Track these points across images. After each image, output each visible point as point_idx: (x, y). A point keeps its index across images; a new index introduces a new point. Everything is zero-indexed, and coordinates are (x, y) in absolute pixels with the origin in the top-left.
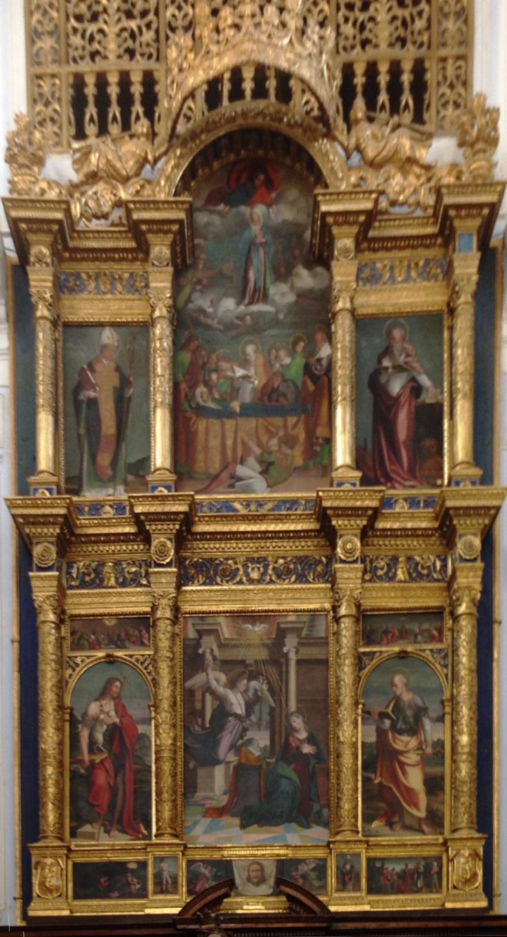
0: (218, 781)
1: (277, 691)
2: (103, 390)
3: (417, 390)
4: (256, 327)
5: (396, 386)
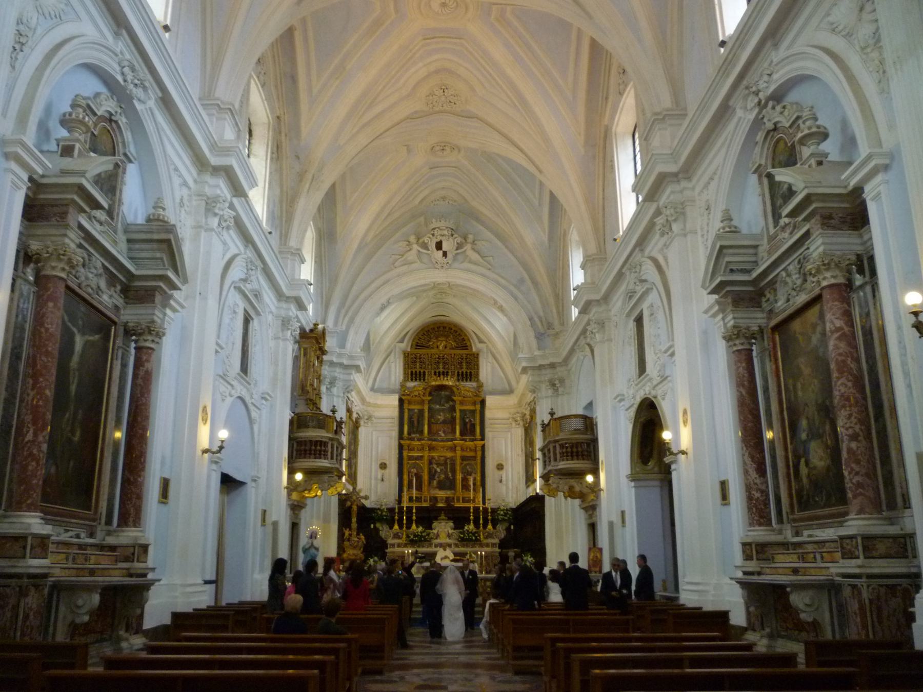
0: (435, 482)
1: (446, 468)
2: (415, 419)
3: (470, 421)
4: (443, 410)
5: (467, 420)
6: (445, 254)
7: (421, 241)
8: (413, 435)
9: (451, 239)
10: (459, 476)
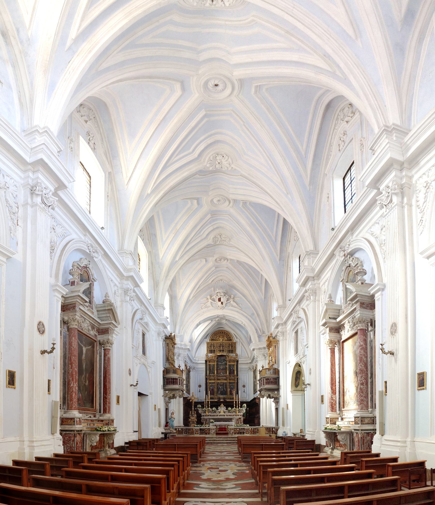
2: (212, 368)
3: (233, 369)
4: (222, 365)
6: (222, 303)
7: (212, 298)
8: (211, 374)
9: (224, 297)
10: (229, 390)
